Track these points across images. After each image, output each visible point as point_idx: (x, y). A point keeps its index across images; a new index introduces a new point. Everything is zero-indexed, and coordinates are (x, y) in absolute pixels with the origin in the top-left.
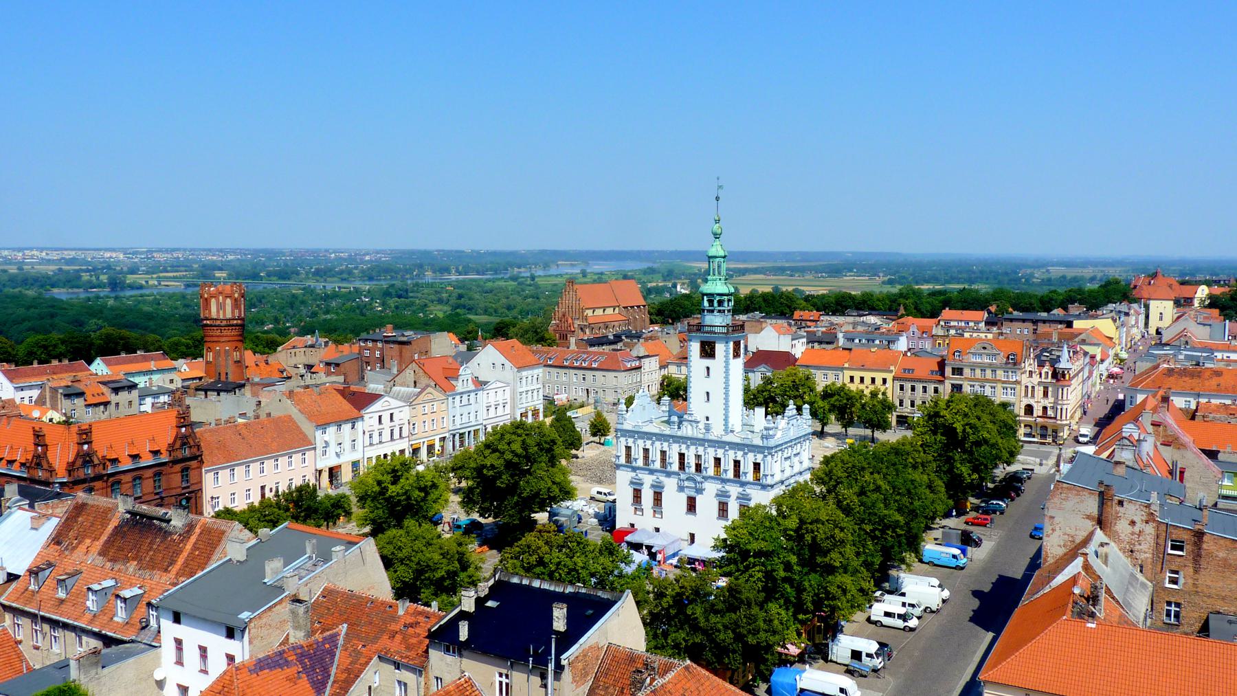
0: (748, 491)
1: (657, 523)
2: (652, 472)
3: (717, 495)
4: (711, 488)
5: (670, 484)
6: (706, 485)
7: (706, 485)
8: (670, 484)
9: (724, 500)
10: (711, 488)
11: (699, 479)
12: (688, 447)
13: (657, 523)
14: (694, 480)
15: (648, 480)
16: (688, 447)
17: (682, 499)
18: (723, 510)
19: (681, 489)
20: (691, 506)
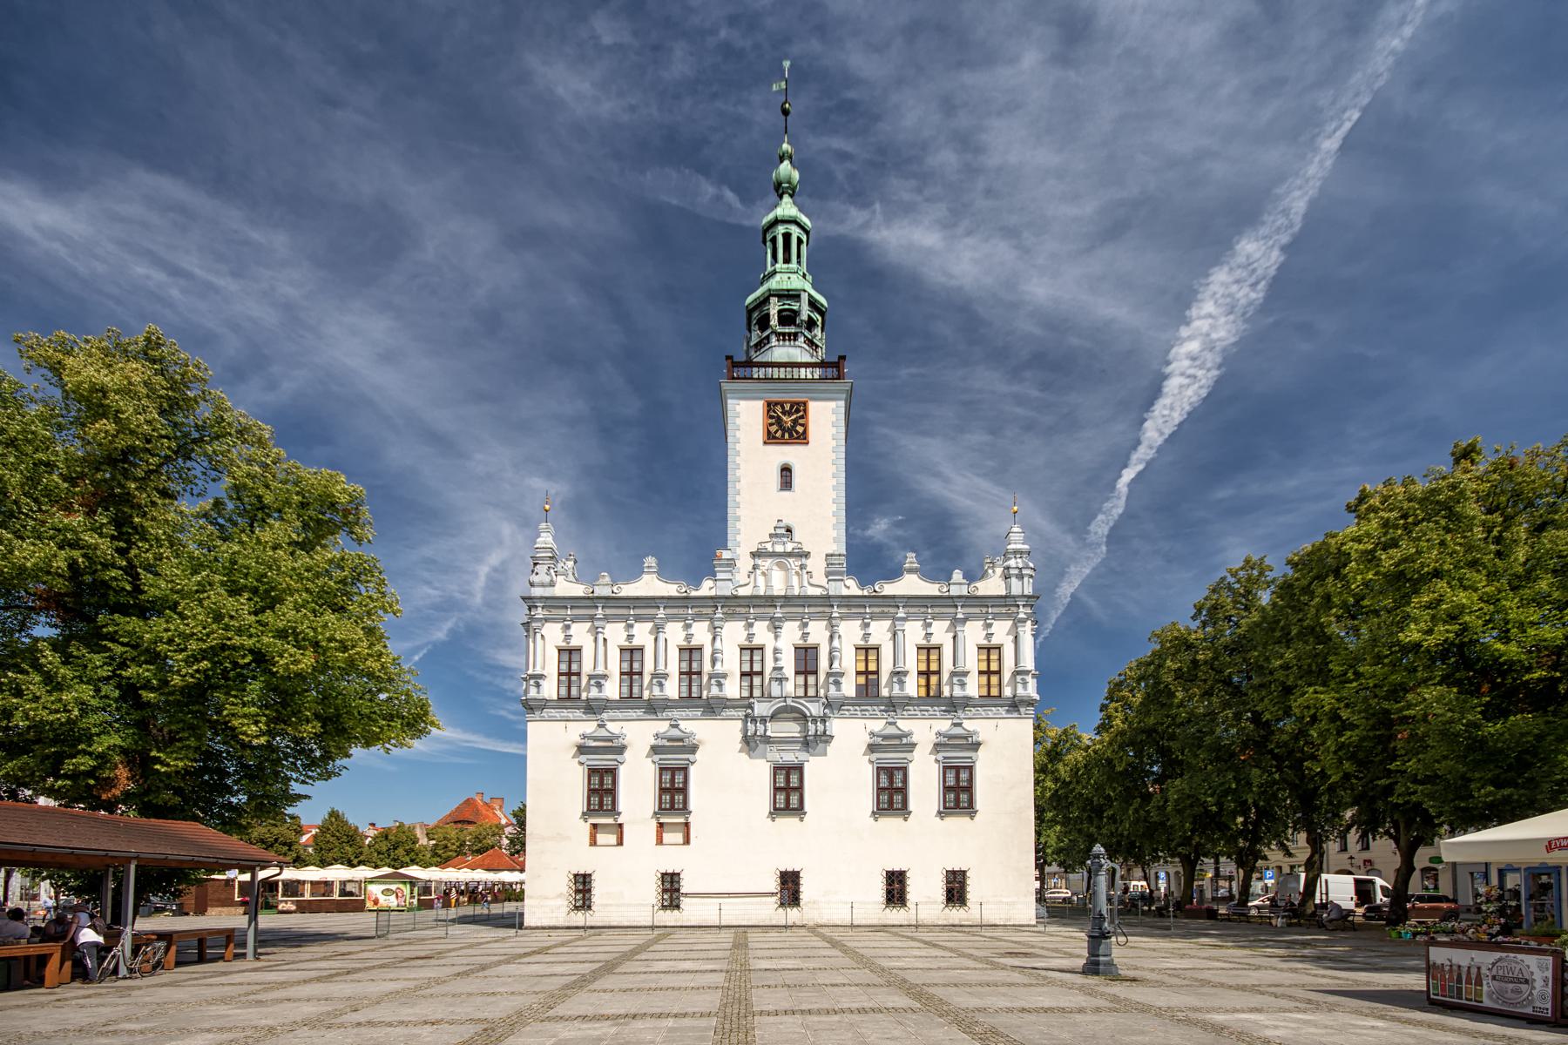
0: (969, 725)
1: (672, 857)
2: (654, 708)
3: (872, 748)
4: (852, 734)
5: (717, 740)
6: (836, 726)
7: (836, 726)
8: (717, 740)
9: (891, 758)
10: (852, 734)
11: (815, 709)
12: (775, 628)
13: (672, 857)
14: (803, 718)
15: (639, 734)
16: (775, 628)
17: (758, 774)
18: (891, 795)
19: (750, 743)
20: (788, 794)
